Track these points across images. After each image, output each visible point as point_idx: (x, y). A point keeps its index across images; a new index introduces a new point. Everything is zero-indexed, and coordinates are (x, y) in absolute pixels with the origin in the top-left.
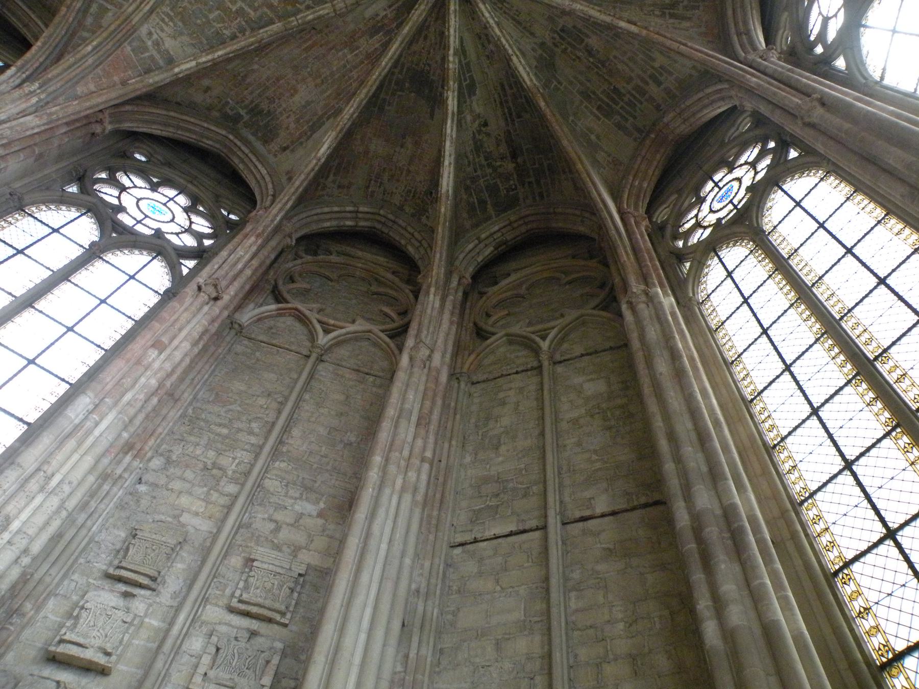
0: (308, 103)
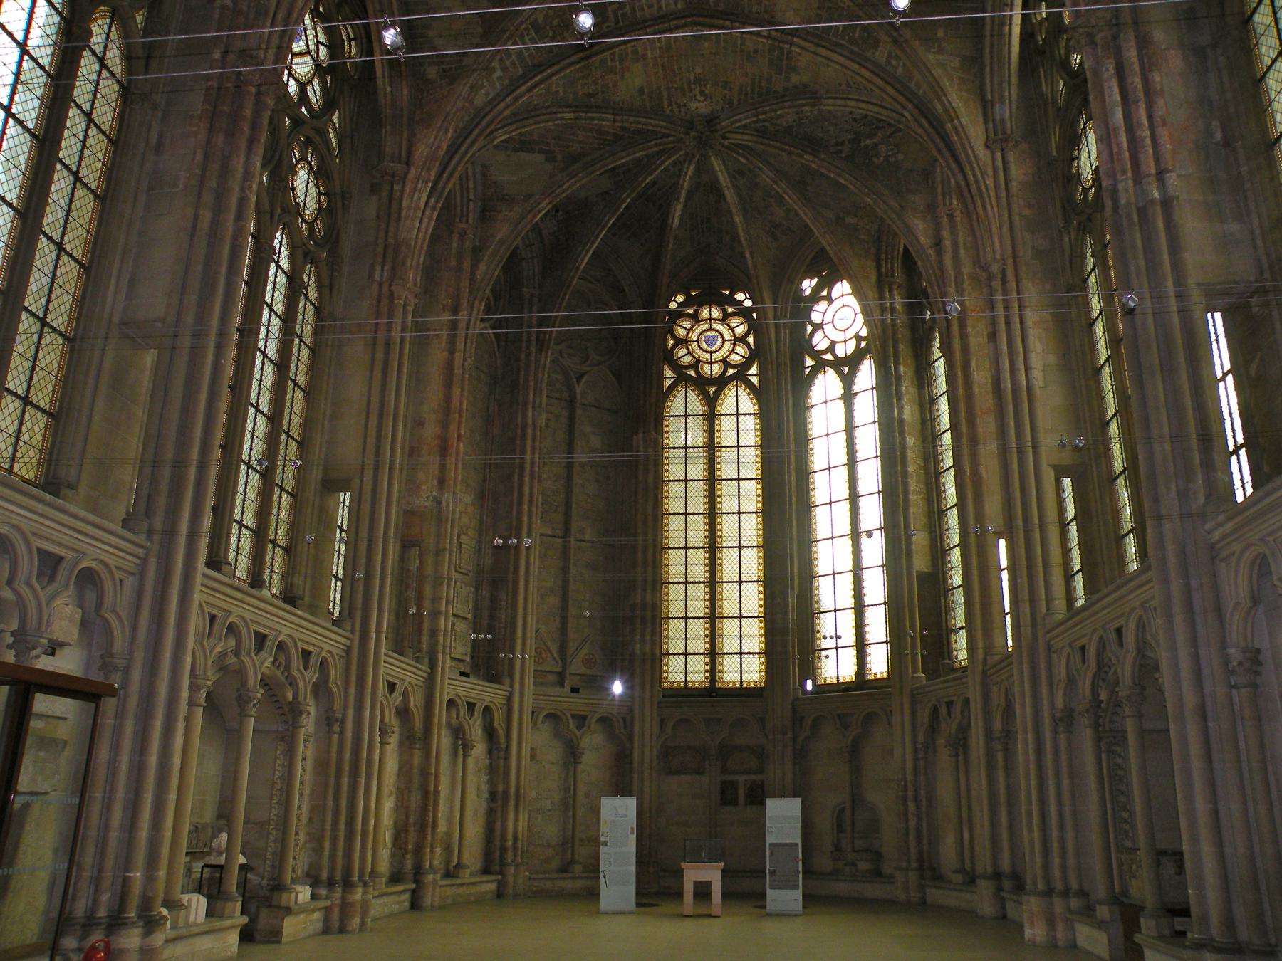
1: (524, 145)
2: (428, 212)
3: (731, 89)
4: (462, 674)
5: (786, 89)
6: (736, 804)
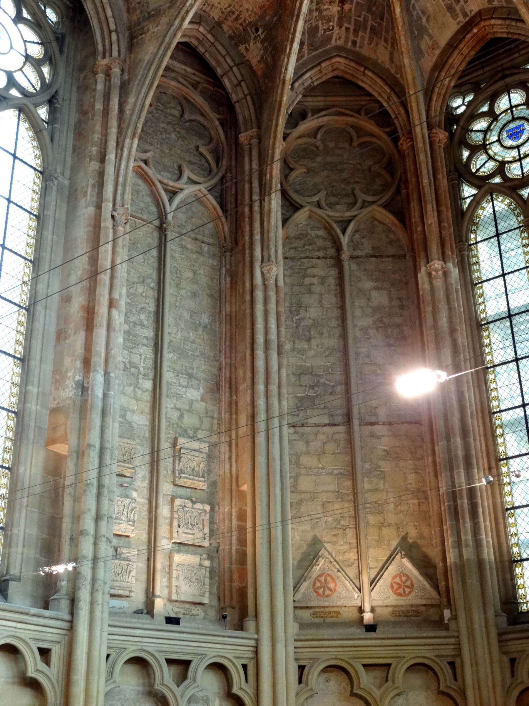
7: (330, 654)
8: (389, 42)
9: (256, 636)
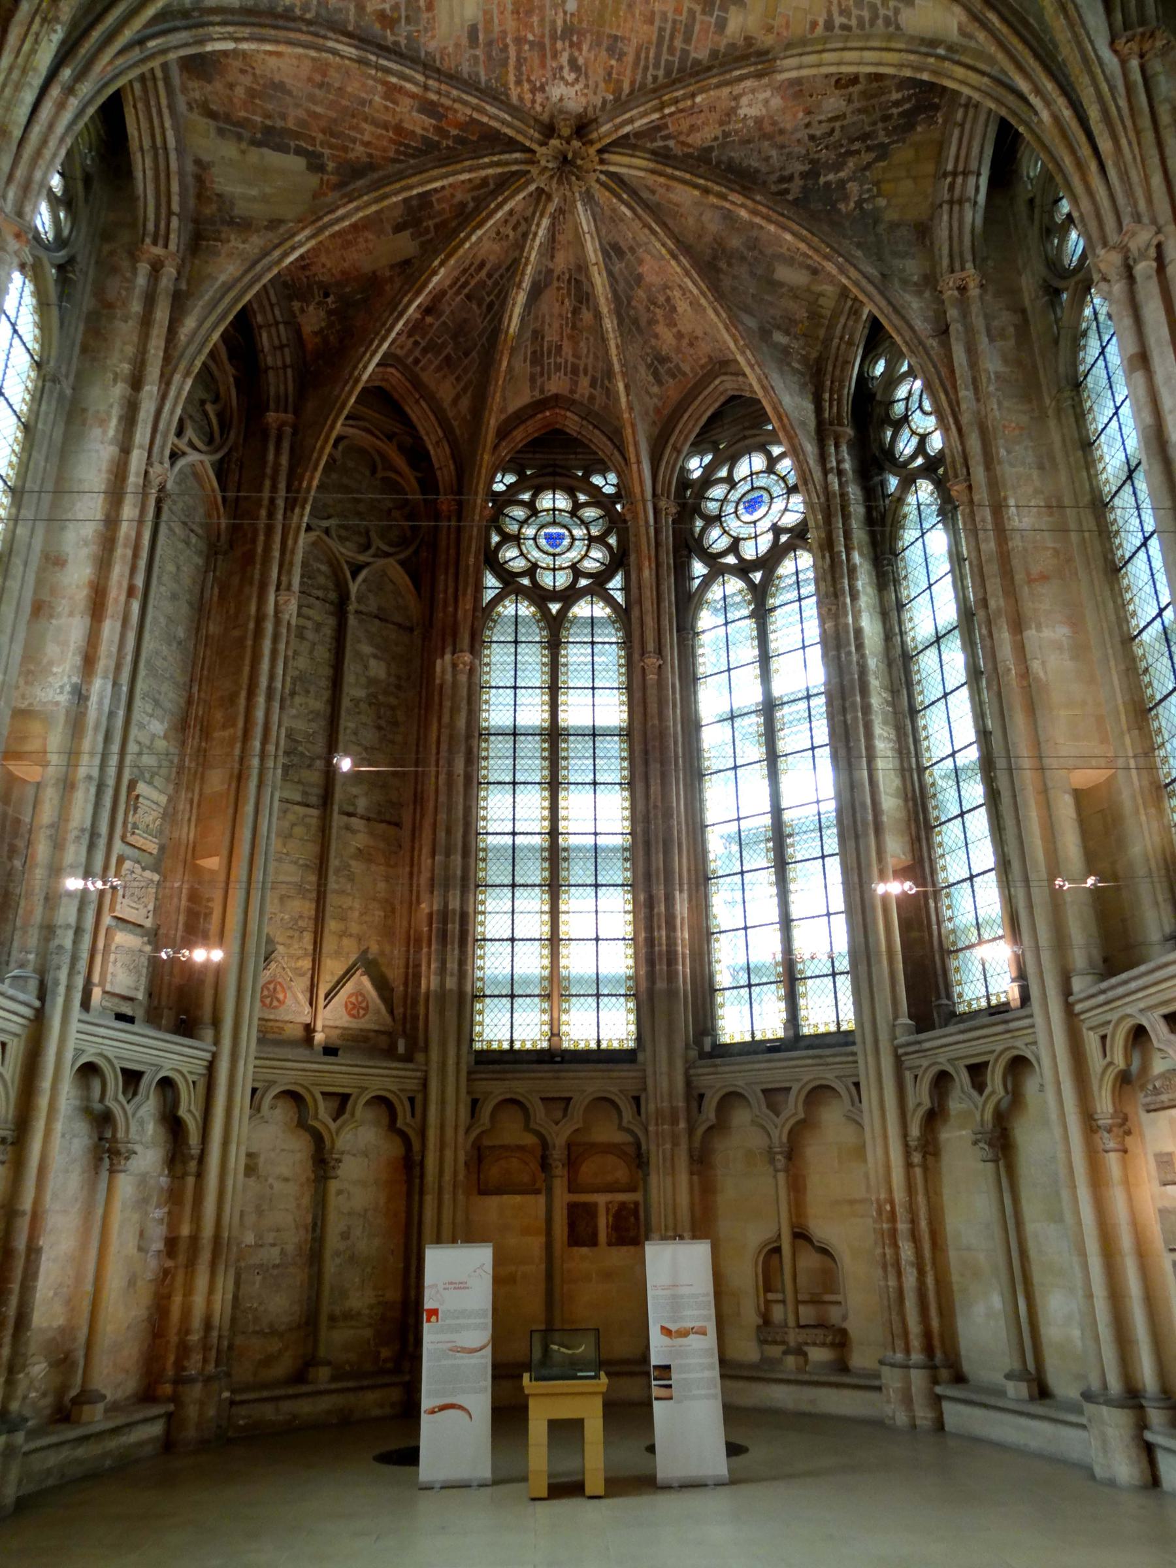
0: (280, 87)
1: (272, 137)
2: (55, 91)
3: (621, 57)
4: (120, 1017)
5: (714, 54)
6: (593, 1242)
7: (287, 1078)
8: (462, 384)
9: (214, 1049)
